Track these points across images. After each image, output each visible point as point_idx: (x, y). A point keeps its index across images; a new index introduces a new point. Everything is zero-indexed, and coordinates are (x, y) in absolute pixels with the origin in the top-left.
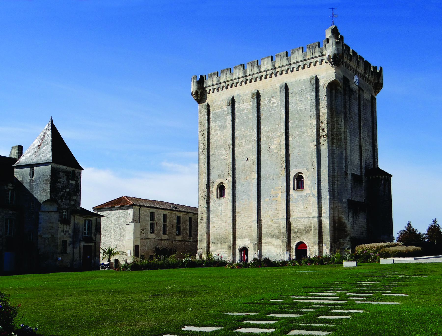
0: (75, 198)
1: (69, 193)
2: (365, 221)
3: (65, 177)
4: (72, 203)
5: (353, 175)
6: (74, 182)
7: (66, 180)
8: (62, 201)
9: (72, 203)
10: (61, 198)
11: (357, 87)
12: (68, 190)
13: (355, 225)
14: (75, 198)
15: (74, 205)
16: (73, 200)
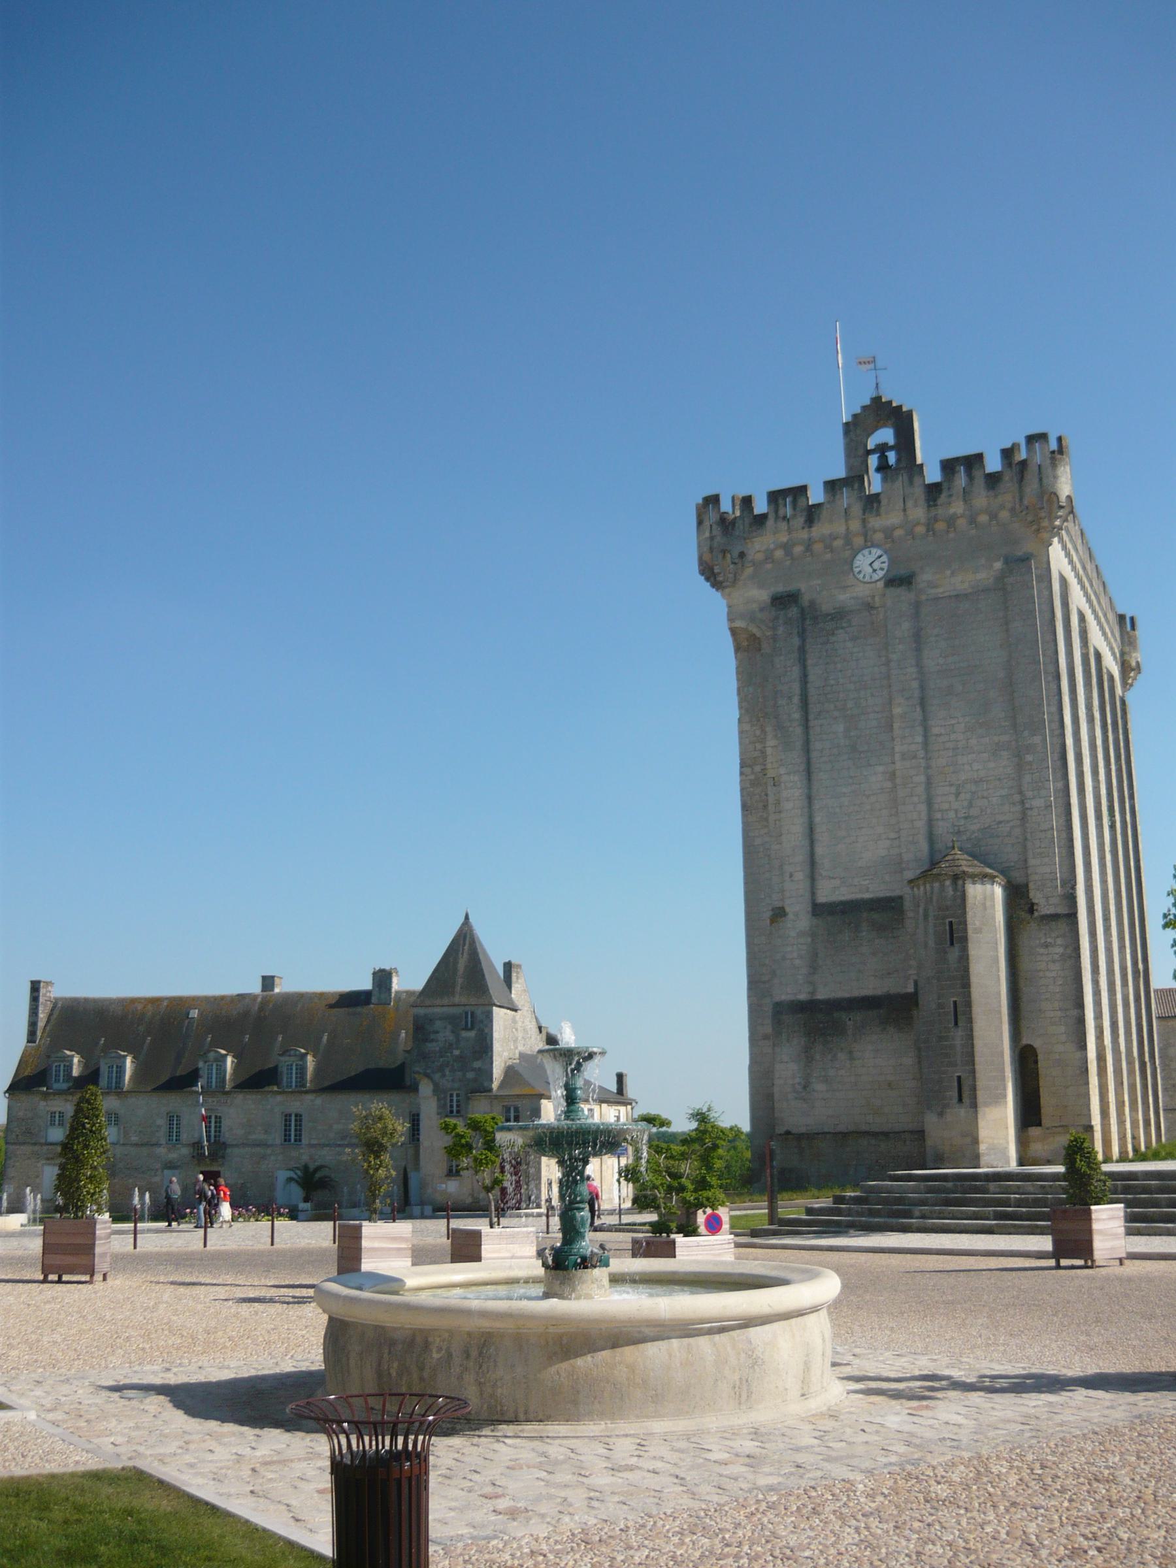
0: (477, 1064)
1: (461, 1058)
2: (909, 1060)
3: (449, 1027)
4: (470, 1075)
5: (819, 910)
6: (472, 1034)
7: (453, 1032)
8: (444, 1076)
9: (470, 1075)
10: (441, 1069)
11: (881, 584)
12: (456, 1052)
13: (820, 1087)
14: (477, 1064)
15: (475, 1080)
16: (473, 1070)
